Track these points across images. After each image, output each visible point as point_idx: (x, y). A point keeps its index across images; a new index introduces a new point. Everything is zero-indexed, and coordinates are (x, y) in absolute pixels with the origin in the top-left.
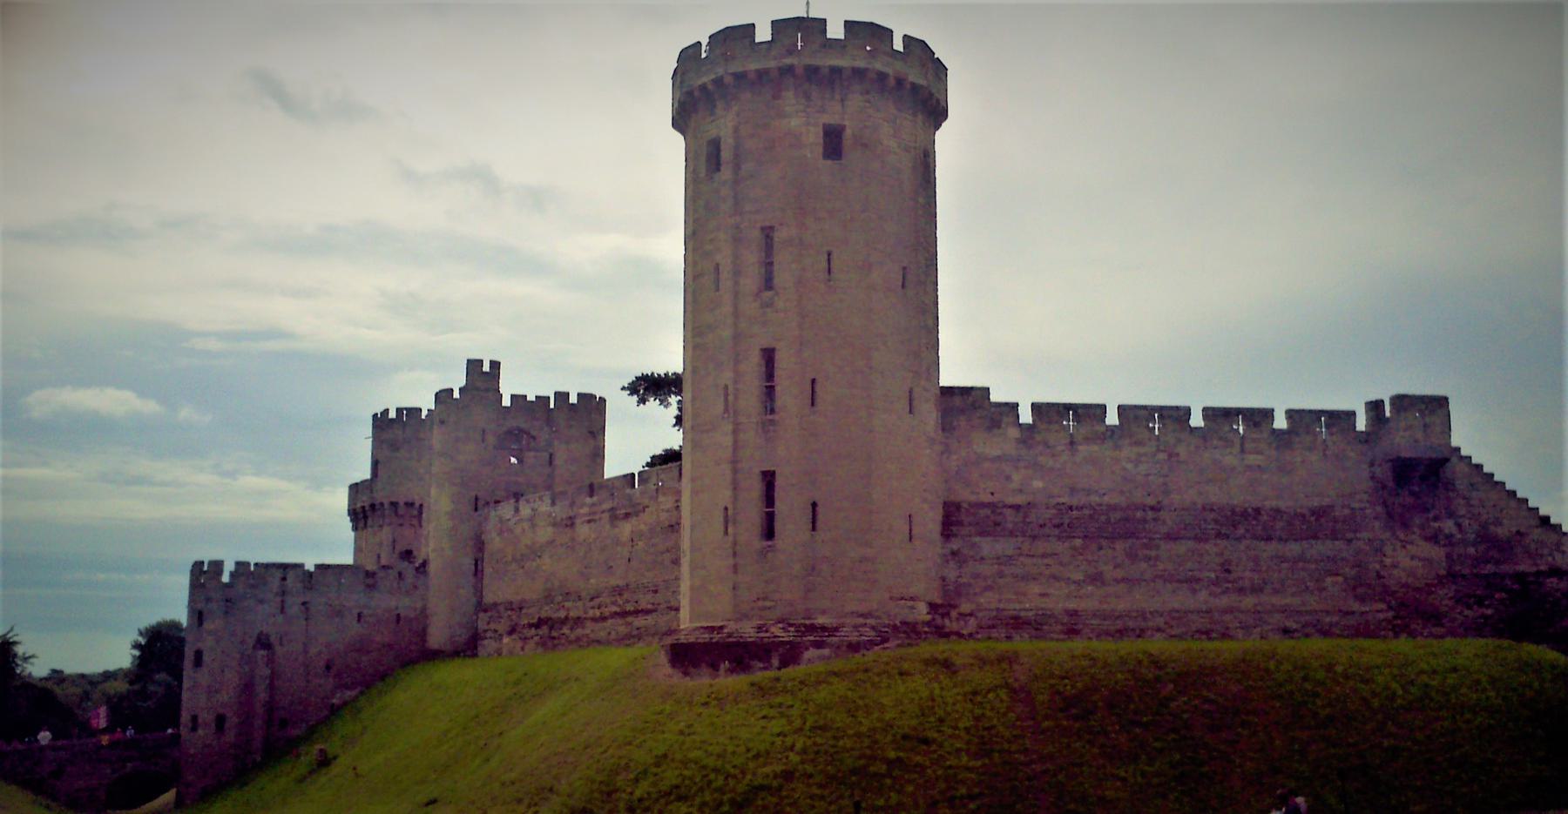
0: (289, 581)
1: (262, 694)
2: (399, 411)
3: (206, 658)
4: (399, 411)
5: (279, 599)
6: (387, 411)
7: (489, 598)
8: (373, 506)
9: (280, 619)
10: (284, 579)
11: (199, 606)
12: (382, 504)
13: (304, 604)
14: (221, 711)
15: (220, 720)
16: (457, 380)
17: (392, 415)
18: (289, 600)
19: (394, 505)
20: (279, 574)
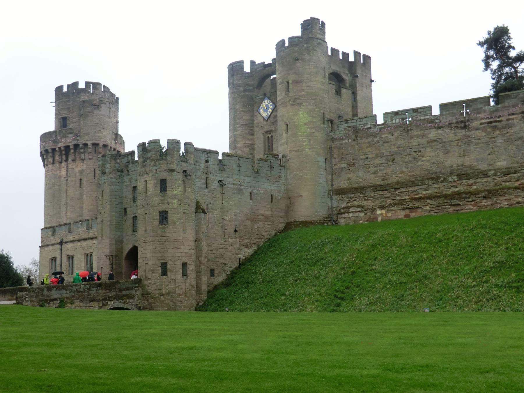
0: (210, 162)
1: (205, 249)
2: (87, 84)
3: (172, 217)
4: (87, 84)
5: (204, 176)
6: (76, 84)
7: (343, 184)
8: (76, 146)
9: (206, 192)
10: (207, 161)
11: (163, 176)
12: (86, 145)
13: (220, 181)
14: (184, 260)
15: (185, 265)
16: (298, 32)
17: (82, 85)
18: (211, 177)
19: (95, 145)
20: (204, 157)
